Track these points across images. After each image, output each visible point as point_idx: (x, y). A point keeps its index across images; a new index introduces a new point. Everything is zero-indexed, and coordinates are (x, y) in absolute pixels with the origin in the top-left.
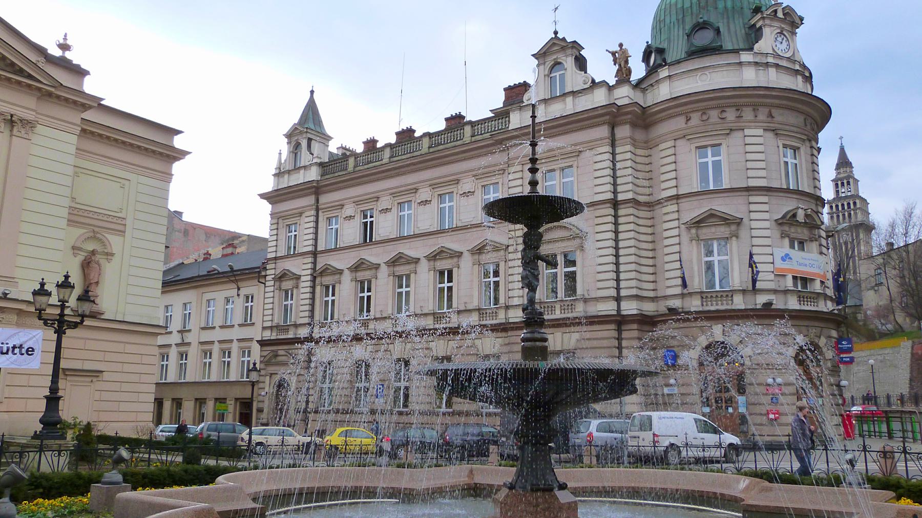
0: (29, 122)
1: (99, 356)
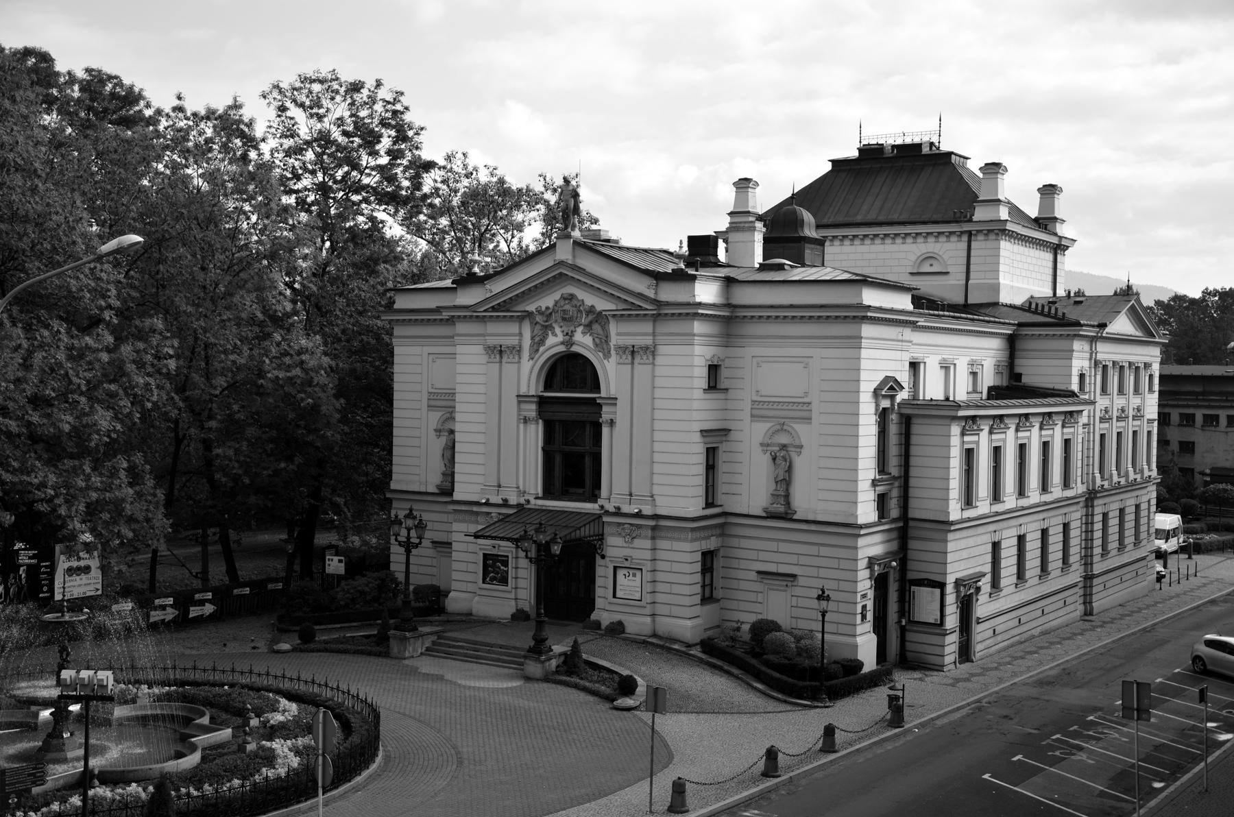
0: (647, 348)
1: (793, 559)
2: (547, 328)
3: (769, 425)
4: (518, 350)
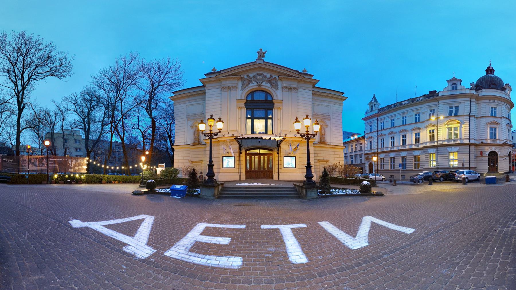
4: (236, 87)
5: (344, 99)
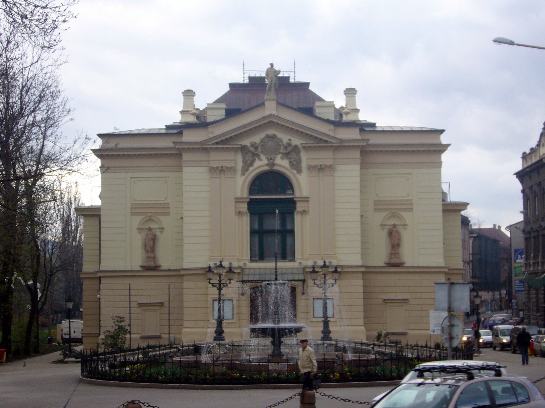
2: (255, 155)
3: (385, 214)
4: (232, 170)
5: (443, 148)
